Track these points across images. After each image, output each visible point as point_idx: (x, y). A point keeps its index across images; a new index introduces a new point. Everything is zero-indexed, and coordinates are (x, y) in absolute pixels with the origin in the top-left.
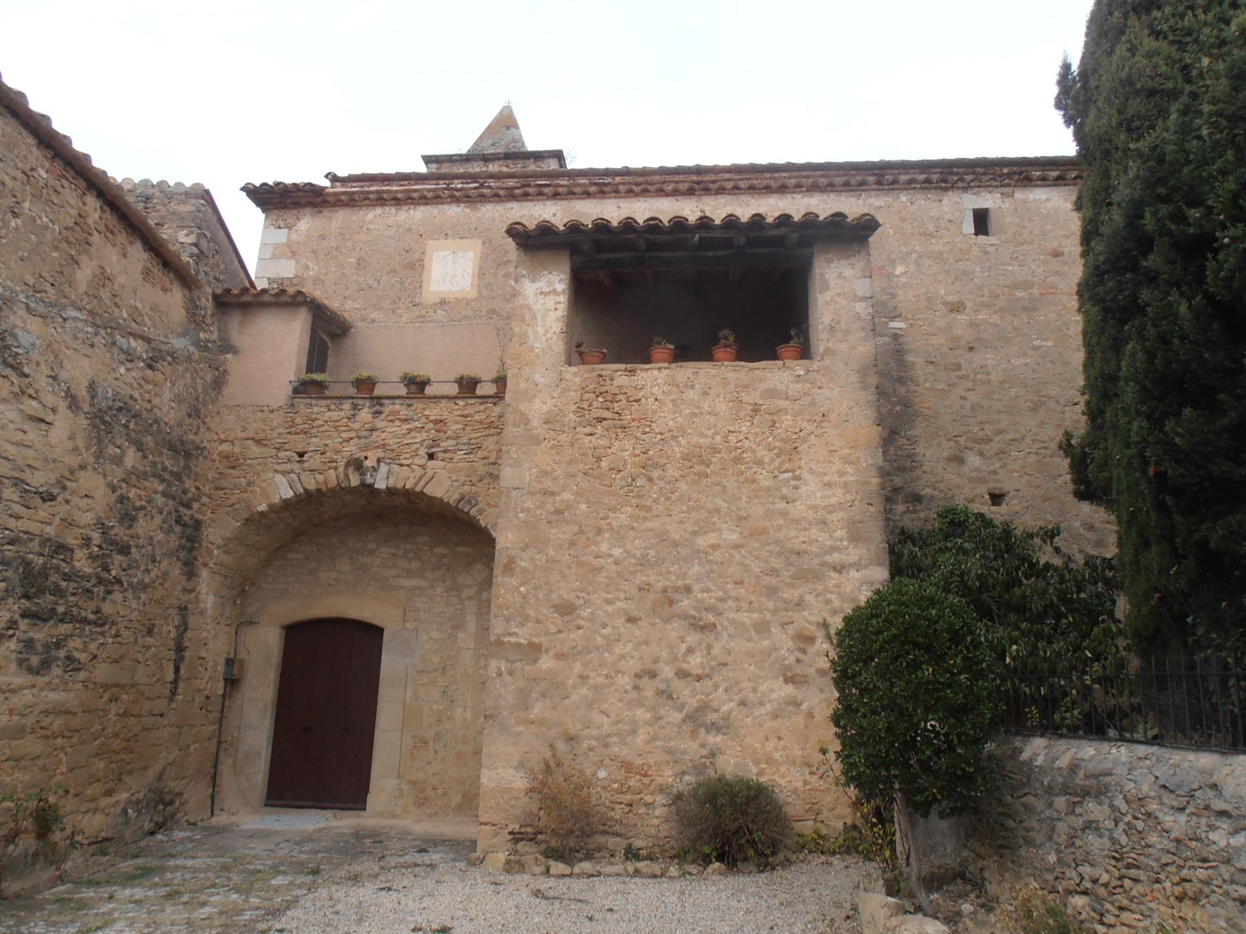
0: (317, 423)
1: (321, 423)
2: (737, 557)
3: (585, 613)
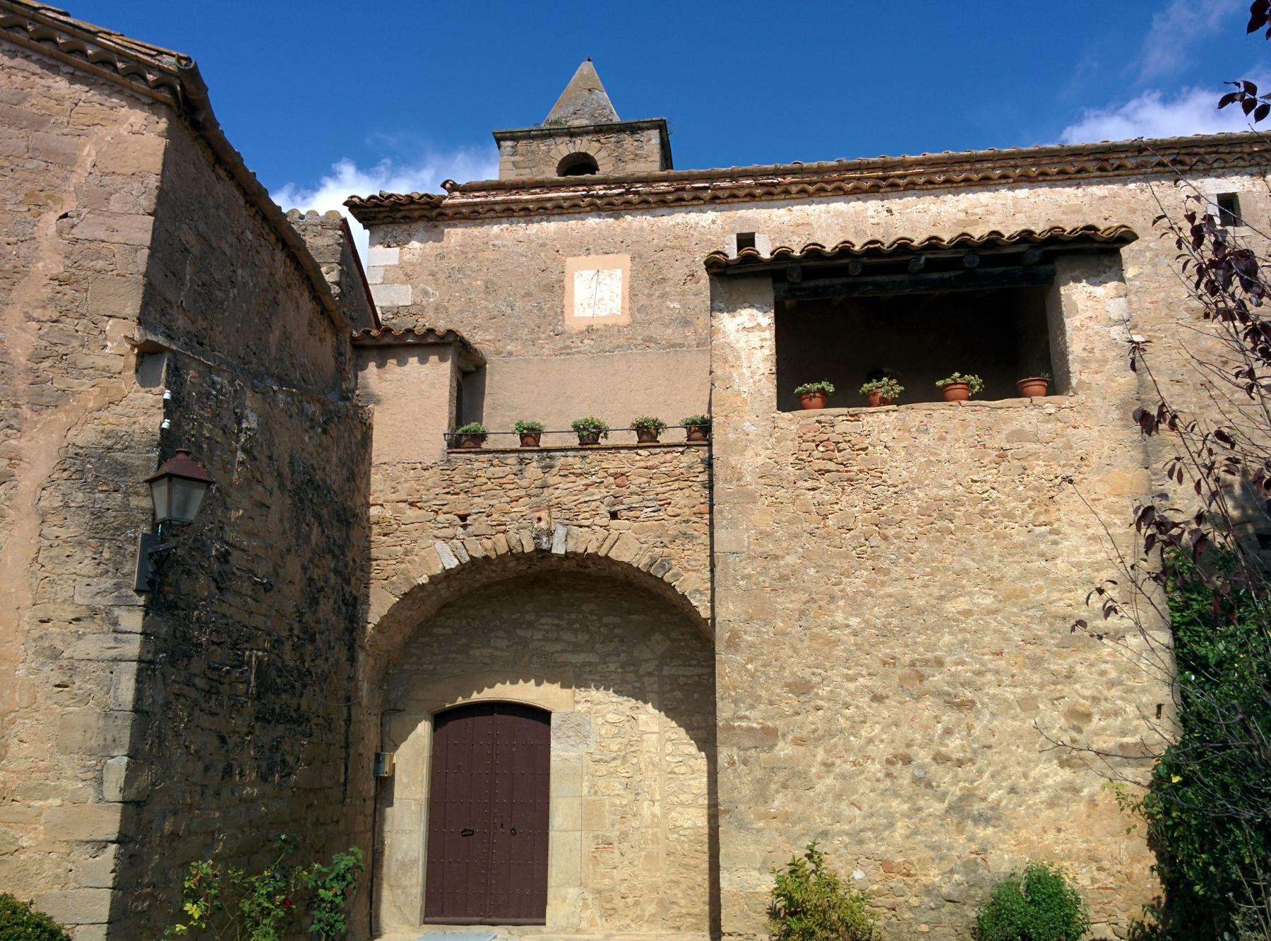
0: (479, 481)
1: (484, 480)
2: (994, 624)
3: (824, 691)
